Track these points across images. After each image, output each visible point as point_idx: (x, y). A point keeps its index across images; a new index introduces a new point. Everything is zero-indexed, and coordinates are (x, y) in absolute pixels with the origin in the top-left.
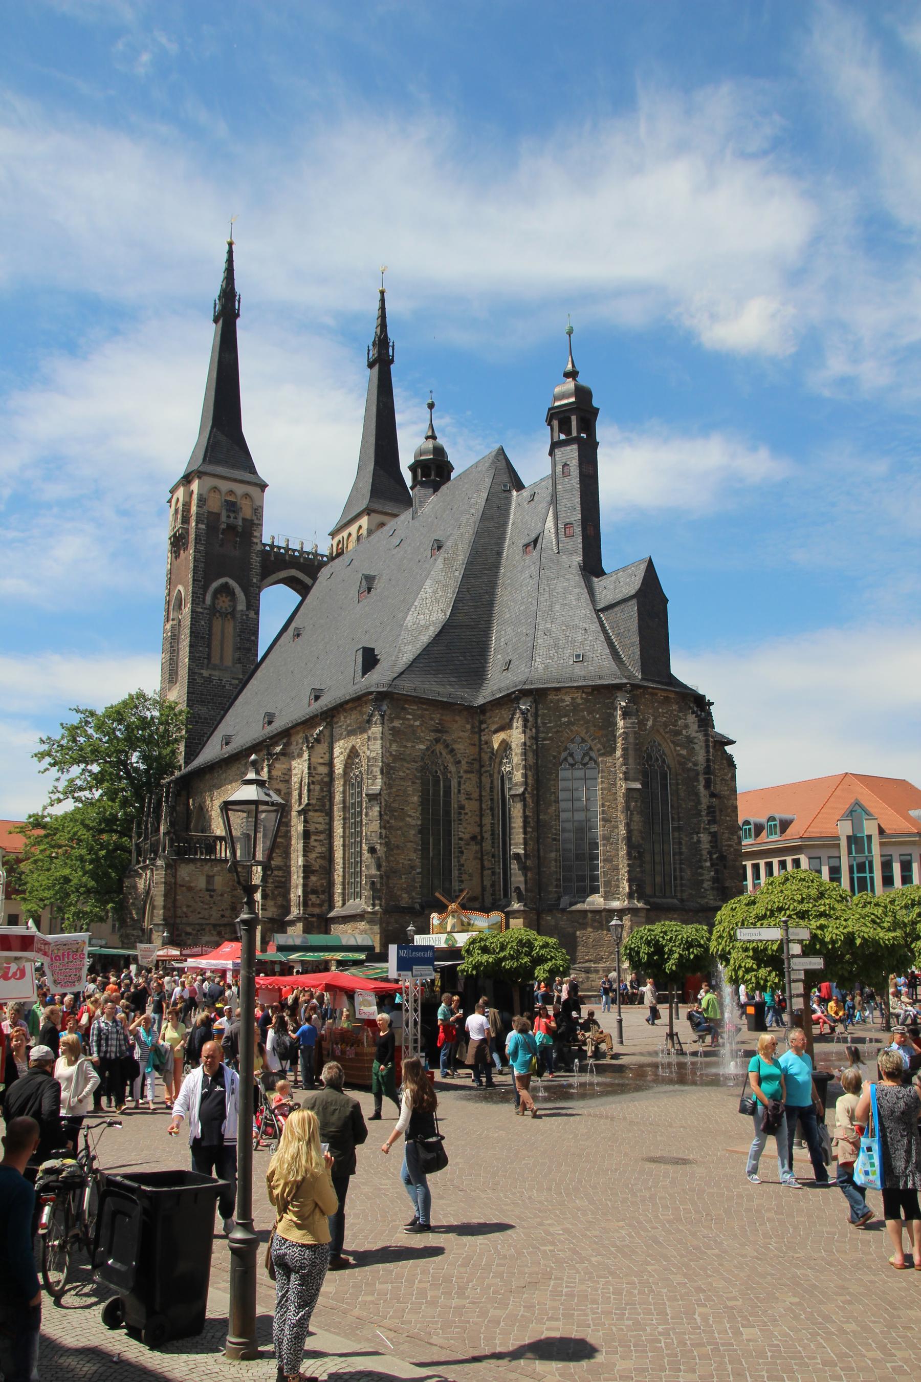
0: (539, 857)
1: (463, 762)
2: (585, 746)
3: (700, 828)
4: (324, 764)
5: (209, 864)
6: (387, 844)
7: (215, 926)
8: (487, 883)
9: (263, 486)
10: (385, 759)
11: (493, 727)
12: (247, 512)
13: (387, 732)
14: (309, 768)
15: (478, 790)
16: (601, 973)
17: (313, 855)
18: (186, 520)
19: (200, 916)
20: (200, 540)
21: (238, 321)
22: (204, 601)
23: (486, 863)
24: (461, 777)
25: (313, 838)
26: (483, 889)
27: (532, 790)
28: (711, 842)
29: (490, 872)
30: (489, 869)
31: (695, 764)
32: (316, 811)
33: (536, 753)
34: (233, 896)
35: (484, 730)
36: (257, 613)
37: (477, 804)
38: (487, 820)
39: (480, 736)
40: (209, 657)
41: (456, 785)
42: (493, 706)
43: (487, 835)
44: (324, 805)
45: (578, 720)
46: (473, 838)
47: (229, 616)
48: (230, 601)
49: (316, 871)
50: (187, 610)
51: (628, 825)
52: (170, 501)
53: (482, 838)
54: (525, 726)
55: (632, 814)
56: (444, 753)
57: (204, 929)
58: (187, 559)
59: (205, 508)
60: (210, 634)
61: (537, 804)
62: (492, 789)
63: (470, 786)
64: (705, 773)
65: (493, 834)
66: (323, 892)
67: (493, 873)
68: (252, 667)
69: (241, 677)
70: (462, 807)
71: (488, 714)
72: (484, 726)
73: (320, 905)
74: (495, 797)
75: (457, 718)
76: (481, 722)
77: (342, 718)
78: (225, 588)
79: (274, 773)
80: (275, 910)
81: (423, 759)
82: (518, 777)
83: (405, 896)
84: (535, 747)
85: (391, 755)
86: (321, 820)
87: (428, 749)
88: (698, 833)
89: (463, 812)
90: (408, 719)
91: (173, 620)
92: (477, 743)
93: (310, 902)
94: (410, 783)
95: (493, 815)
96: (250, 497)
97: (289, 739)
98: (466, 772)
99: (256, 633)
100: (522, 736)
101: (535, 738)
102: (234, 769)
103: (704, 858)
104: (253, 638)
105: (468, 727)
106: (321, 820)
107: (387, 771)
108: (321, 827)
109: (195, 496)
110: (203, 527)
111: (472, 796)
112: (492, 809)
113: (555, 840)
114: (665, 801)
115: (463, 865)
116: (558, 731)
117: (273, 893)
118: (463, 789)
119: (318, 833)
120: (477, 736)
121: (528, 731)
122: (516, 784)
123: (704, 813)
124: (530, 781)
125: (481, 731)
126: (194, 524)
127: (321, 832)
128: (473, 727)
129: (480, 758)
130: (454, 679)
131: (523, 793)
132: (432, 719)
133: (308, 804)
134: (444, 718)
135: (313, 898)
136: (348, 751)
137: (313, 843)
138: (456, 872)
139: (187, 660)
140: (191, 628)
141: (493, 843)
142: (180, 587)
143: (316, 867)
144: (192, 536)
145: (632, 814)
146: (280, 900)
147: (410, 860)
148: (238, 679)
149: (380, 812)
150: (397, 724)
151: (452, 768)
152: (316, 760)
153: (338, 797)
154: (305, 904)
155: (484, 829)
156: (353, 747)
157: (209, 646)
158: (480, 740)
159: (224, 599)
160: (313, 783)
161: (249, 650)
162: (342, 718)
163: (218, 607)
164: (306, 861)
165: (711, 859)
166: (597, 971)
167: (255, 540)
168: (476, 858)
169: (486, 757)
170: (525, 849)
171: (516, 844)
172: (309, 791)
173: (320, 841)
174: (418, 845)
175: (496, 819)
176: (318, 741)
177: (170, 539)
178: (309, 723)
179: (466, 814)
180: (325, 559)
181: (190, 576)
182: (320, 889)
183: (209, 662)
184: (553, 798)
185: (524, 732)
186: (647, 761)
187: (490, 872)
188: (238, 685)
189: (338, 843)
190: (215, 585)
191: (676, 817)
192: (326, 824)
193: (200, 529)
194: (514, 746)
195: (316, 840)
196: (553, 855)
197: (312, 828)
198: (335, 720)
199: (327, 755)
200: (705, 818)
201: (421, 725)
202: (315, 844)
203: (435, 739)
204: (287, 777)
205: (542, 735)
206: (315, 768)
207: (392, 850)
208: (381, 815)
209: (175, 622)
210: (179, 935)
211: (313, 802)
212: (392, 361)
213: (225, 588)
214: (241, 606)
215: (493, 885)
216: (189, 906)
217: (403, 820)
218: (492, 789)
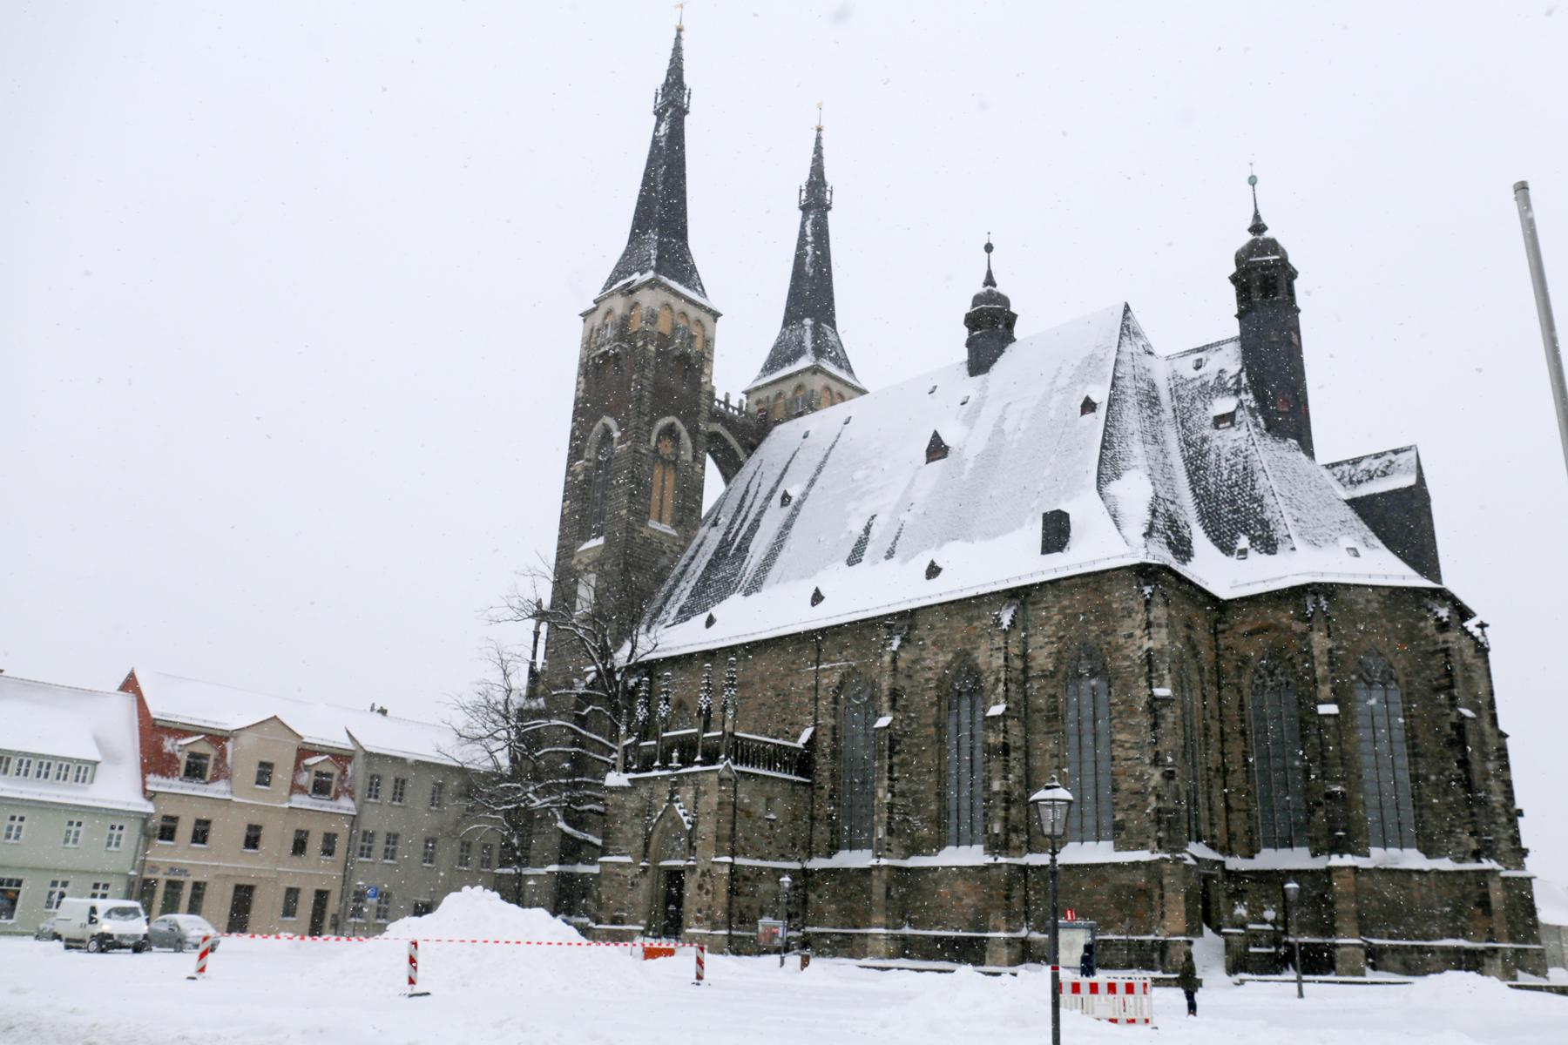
9: (716, 315)
11: (1245, 629)
21: (687, 118)
23: (1233, 803)
25: (1013, 755)
35: (1223, 631)
46: (1218, 770)
72: (1220, 627)
76: (1218, 621)
78: (670, 431)
96: (703, 326)
99: (701, 491)
112: (1243, 733)
158: (1217, 647)
161: (692, 511)
190: (663, 422)
197: (1011, 742)
211: (1011, 705)
212: (829, 208)
213: (670, 431)
214: (687, 455)
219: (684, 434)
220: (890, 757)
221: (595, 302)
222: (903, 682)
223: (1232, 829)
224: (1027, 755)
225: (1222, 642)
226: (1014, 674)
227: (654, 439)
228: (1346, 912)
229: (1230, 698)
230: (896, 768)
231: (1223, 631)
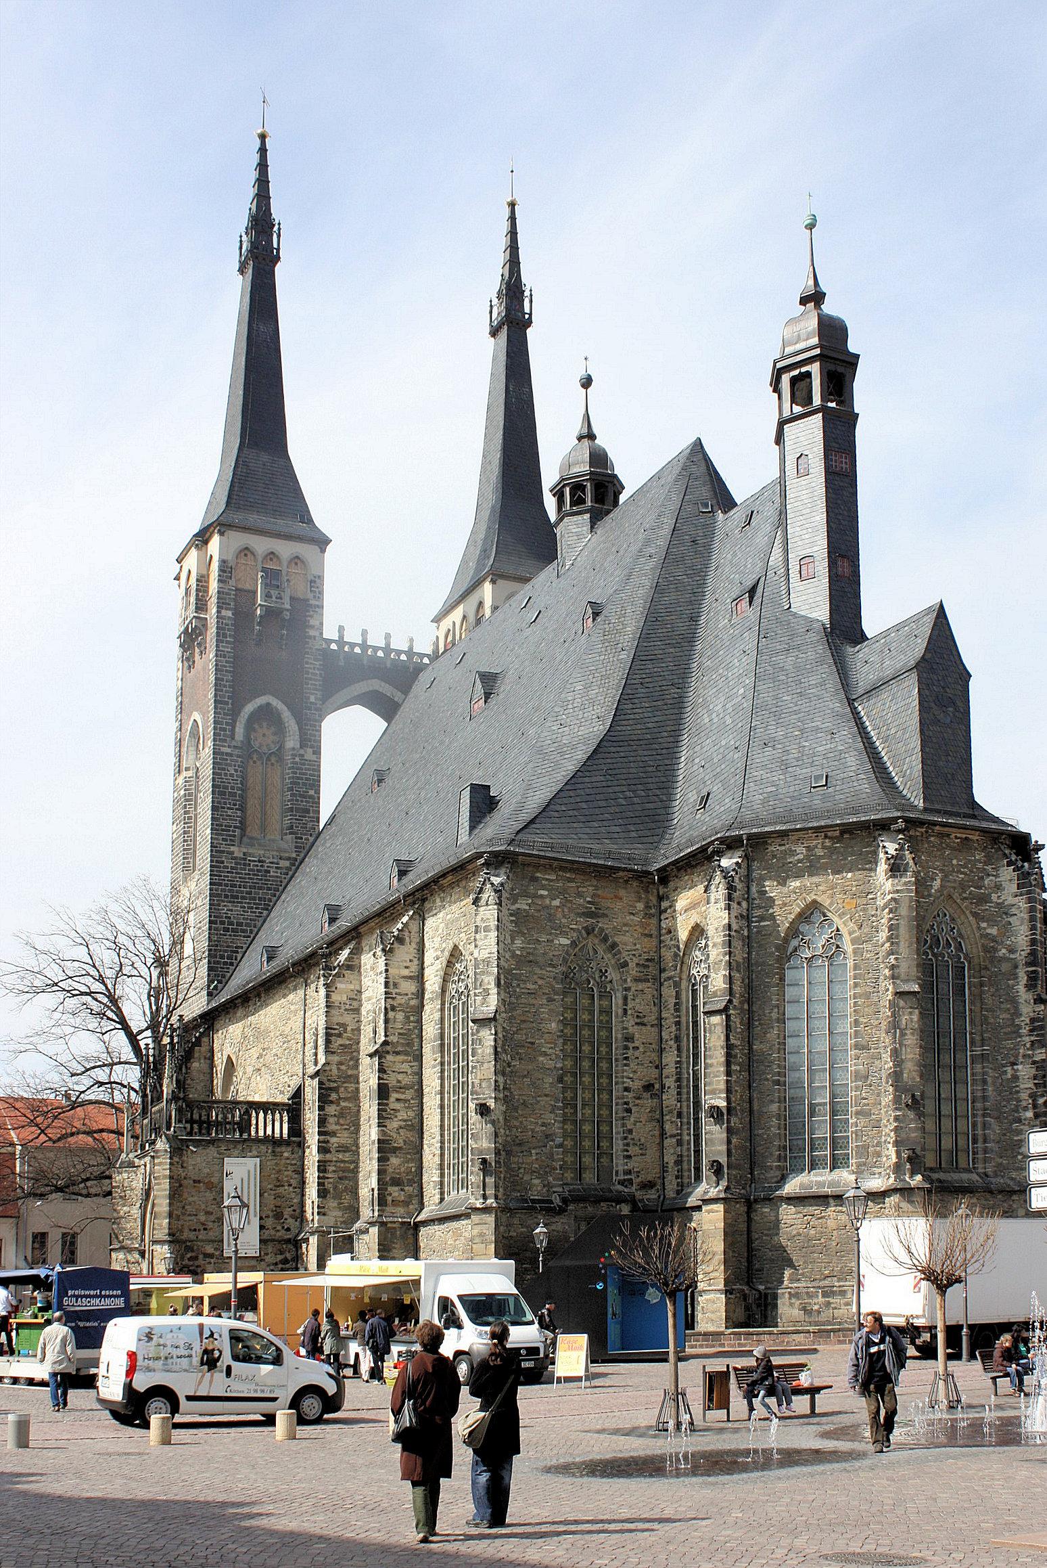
0: (751, 1111)
3: (1017, 1056)
4: (411, 978)
5: (240, 1147)
6: (506, 1100)
10: (502, 963)
12: (301, 590)
13: (506, 919)
14: (387, 984)
17: (393, 1125)
18: (201, 606)
20: (225, 636)
22: (233, 737)
24: (627, 989)
25: (394, 1096)
27: (741, 1003)
31: (1012, 951)
32: (397, 1053)
33: (748, 941)
34: (277, 1196)
35: (665, 911)
36: (317, 752)
40: (243, 826)
41: (620, 1002)
42: (679, 869)
44: (410, 1044)
48: (275, 734)
49: (400, 1148)
50: (207, 752)
51: (895, 1053)
52: (177, 578)
53: (663, 1086)
54: (730, 898)
55: (903, 1035)
56: (601, 952)
58: (205, 668)
59: (232, 582)
60: (244, 790)
61: (749, 1025)
64: (1028, 964)
68: (311, 839)
69: (294, 855)
70: (629, 1038)
71: (671, 885)
72: (665, 904)
73: (406, 1203)
75: (622, 893)
76: (661, 898)
77: (438, 900)
78: (266, 715)
79: (335, 997)
80: (340, 1214)
81: (565, 960)
82: (718, 982)
84: (746, 934)
85: (514, 955)
86: (405, 1067)
87: (574, 944)
88: (1014, 1064)
89: (631, 1045)
90: (542, 896)
91: (187, 769)
92: (654, 932)
93: (389, 1199)
94: (545, 1002)
97: (359, 943)
98: (636, 980)
99: (315, 784)
100: (725, 914)
101: (747, 918)
103: (1024, 1103)
104: (312, 792)
105: (640, 906)
106: (405, 1067)
107: (505, 982)
108: (406, 1080)
109: (215, 566)
110: (229, 614)
113: (778, 1083)
114: (960, 1015)
117: (335, 1188)
118: (629, 1003)
119: (401, 1088)
120: (654, 921)
121: (734, 905)
122: (715, 994)
124: (736, 988)
125: (661, 912)
126: (214, 610)
127: (406, 1087)
128: (647, 907)
130: (617, 829)
131: (726, 1009)
132: (579, 895)
133: (385, 1043)
134: (599, 892)
135: (394, 1191)
136: (447, 954)
137: (393, 1104)
139: (209, 831)
140: (214, 779)
142: (196, 716)
143: (399, 1143)
144: (212, 631)
145: (903, 1035)
147: (543, 1125)
148: (289, 859)
149: (496, 1048)
150: (523, 904)
151: (612, 974)
152: (397, 971)
153: (430, 1030)
154: (382, 1202)
156: (456, 947)
157: (242, 809)
159: (265, 731)
160: (393, 1008)
161: (308, 811)
162: (438, 900)
163: (256, 745)
164: (383, 1133)
167: (312, 633)
170: (728, 1100)
171: (713, 1092)
172: (386, 1021)
173: (405, 1101)
174: (557, 1100)
176: (400, 940)
177: (180, 637)
178: (387, 913)
180: (426, 661)
181: (211, 695)
182: (405, 1178)
183: (242, 836)
184: (774, 1015)
185: (729, 908)
186: (930, 947)
188: (289, 869)
189: (431, 1103)
190: (249, 708)
191: (978, 1038)
193: (223, 618)
194: (711, 931)
195: (398, 1100)
196: (774, 1107)
197: (392, 1080)
198: (427, 905)
199: (416, 962)
200: (1027, 1039)
201: (563, 905)
202: (398, 1106)
203: (586, 928)
204: (355, 1004)
205: (757, 913)
206: (395, 985)
207: (516, 1109)
208: (496, 1053)
209: (190, 773)
210: (196, 1258)
211: (393, 1039)
216: (208, 1213)
217: (532, 1060)
219: (286, 714)
220: (321, 1108)
221: (179, 561)
222: (348, 1019)
226: (401, 999)
227: (240, 730)
230: (331, 1120)
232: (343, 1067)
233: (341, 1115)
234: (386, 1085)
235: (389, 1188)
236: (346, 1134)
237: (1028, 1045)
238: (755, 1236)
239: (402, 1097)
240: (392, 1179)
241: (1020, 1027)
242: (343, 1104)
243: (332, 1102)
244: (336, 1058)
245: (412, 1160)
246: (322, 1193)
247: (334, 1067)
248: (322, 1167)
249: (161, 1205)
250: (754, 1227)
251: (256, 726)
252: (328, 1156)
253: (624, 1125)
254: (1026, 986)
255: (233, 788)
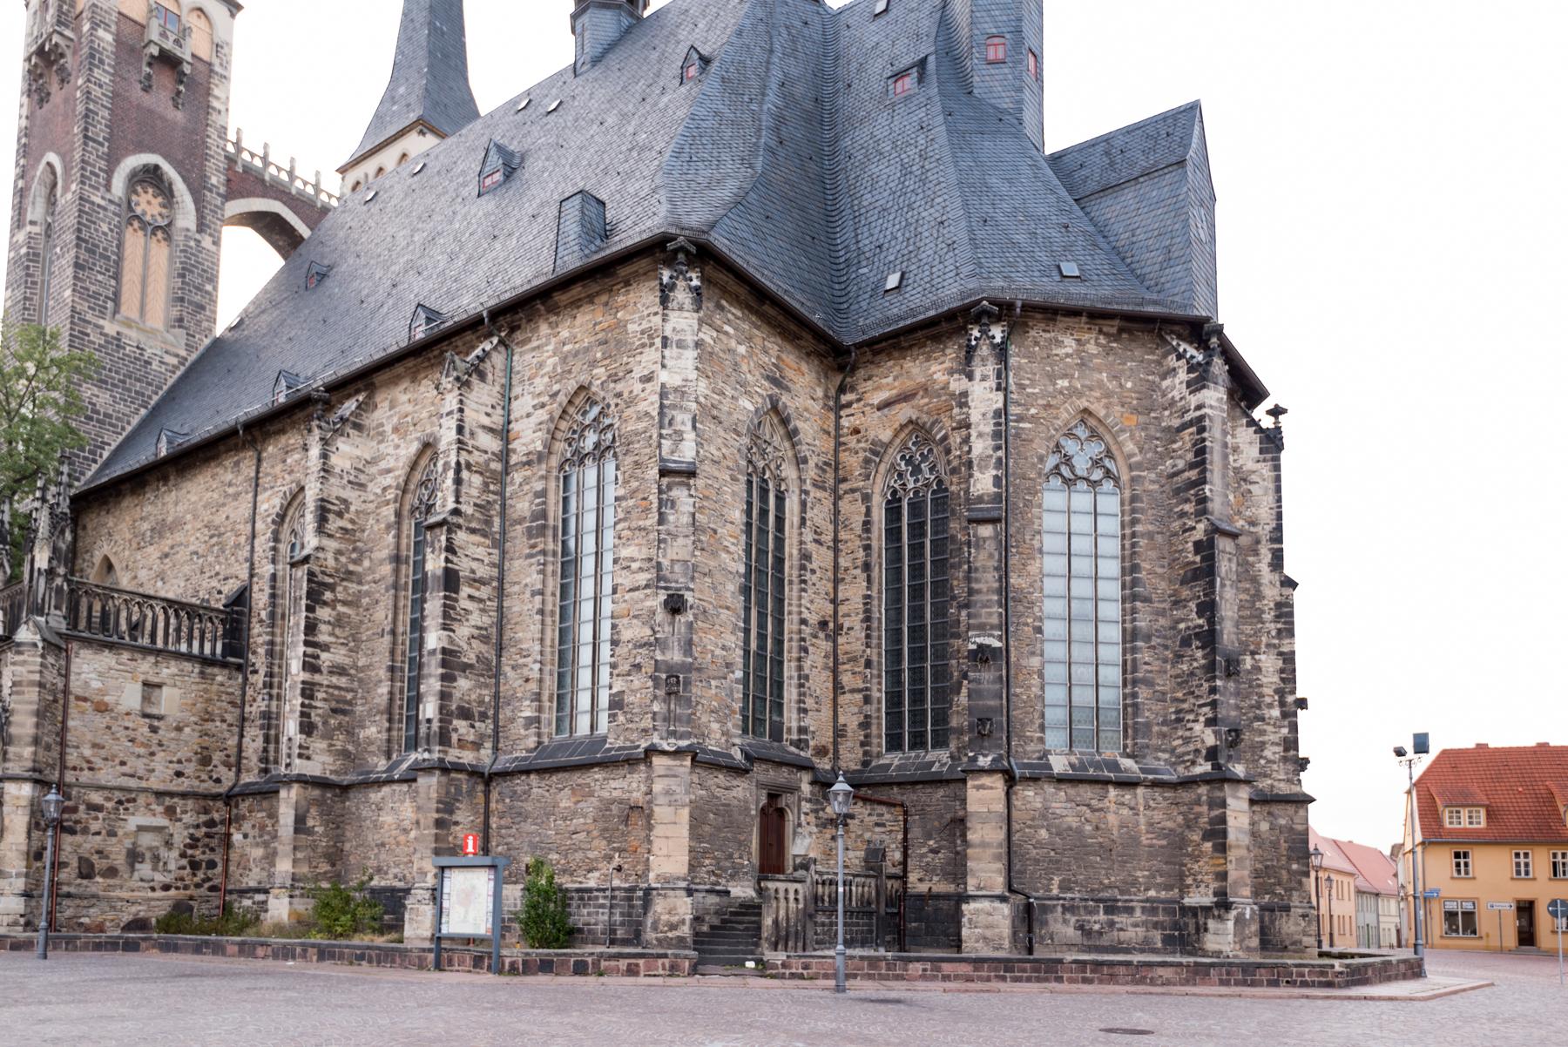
1: (811, 463)
2: (1095, 449)
3: (1258, 644)
7: (159, 795)
8: (849, 719)
11: (878, 398)
15: (831, 527)
16: (1138, 913)
17: (463, 631)
19: (125, 769)
23: (846, 679)
24: (807, 493)
26: (839, 733)
28: (1282, 671)
29: (859, 697)
30: (853, 691)
35: (849, 405)
37: (831, 554)
38: (853, 592)
39: (839, 417)
41: (796, 508)
43: (854, 622)
45: (1091, 389)
46: (823, 624)
47: (160, 234)
48: (164, 206)
49: (471, 666)
57: (134, 800)
62: (867, 526)
63: (819, 515)
65: (868, 619)
66: (483, 716)
67: (867, 700)
71: (861, 373)
72: (845, 398)
73: (477, 746)
74: (875, 544)
76: (842, 389)
83: (715, 726)
91: (32, 223)
93: (455, 737)
95: (869, 580)
102: (201, 479)
105: (820, 393)
108: (483, 571)
111: (823, 538)
112: (867, 567)
115: (807, 678)
116: (1048, 406)
117: (325, 723)
120: (832, 416)
123: (1267, 617)
128: (826, 396)
129: (837, 463)
135: (461, 725)
138: (794, 691)
139: (68, 293)
141: (868, 636)
143: (470, 658)
146: (340, 741)
147: (724, 648)
151: (789, 471)
155: (842, 609)
157: (117, 277)
158: (838, 427)
159: (149, 197)
165: (1282, 704)
166: (1130, 911)
168: (826, 667)
169: (852, 462)
173: (481, 601)
175: (875, 587)
179: (813, 572)
182: (476, 710)
187: (859, 697)
192: (493, 565)
195: (470, 597)
200: (1272, 626)
209: (36, 229)
210: (75, 810)
214: (186, 218)
215: (865, 725)
217: (714, 554)
218: (867, 526)
219: (180, 187)
220: (310, 609)
223: (842, 720)
224: (501, 593)
225: (845, 422)
228: (984, 845)
229: (852, 510)
230: (323, 628)
231: (849, 405)
232: (343, 559)
233: (339, 622)
234: (456, 572)
235: (455, 722)
236: (343, 651)
237: (1274, 633)
238: (1015, 826)
239: (477, 594)
240: (460, 708)
241: (1263, 612)
242: (340, 608)
243: (325, 603)
244: (332, 545)
245: (486, 686)
246: (307, 728)
247: (330, 556)
248: (308, 691)
249: (22, 725)
250: (1015, 813)
251: (139, 189)
252: (317, 678)
253: (800, 668)
254: (1270, 565)
255: (105, 249)
